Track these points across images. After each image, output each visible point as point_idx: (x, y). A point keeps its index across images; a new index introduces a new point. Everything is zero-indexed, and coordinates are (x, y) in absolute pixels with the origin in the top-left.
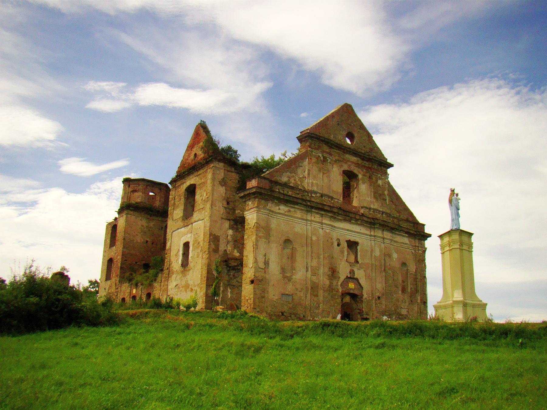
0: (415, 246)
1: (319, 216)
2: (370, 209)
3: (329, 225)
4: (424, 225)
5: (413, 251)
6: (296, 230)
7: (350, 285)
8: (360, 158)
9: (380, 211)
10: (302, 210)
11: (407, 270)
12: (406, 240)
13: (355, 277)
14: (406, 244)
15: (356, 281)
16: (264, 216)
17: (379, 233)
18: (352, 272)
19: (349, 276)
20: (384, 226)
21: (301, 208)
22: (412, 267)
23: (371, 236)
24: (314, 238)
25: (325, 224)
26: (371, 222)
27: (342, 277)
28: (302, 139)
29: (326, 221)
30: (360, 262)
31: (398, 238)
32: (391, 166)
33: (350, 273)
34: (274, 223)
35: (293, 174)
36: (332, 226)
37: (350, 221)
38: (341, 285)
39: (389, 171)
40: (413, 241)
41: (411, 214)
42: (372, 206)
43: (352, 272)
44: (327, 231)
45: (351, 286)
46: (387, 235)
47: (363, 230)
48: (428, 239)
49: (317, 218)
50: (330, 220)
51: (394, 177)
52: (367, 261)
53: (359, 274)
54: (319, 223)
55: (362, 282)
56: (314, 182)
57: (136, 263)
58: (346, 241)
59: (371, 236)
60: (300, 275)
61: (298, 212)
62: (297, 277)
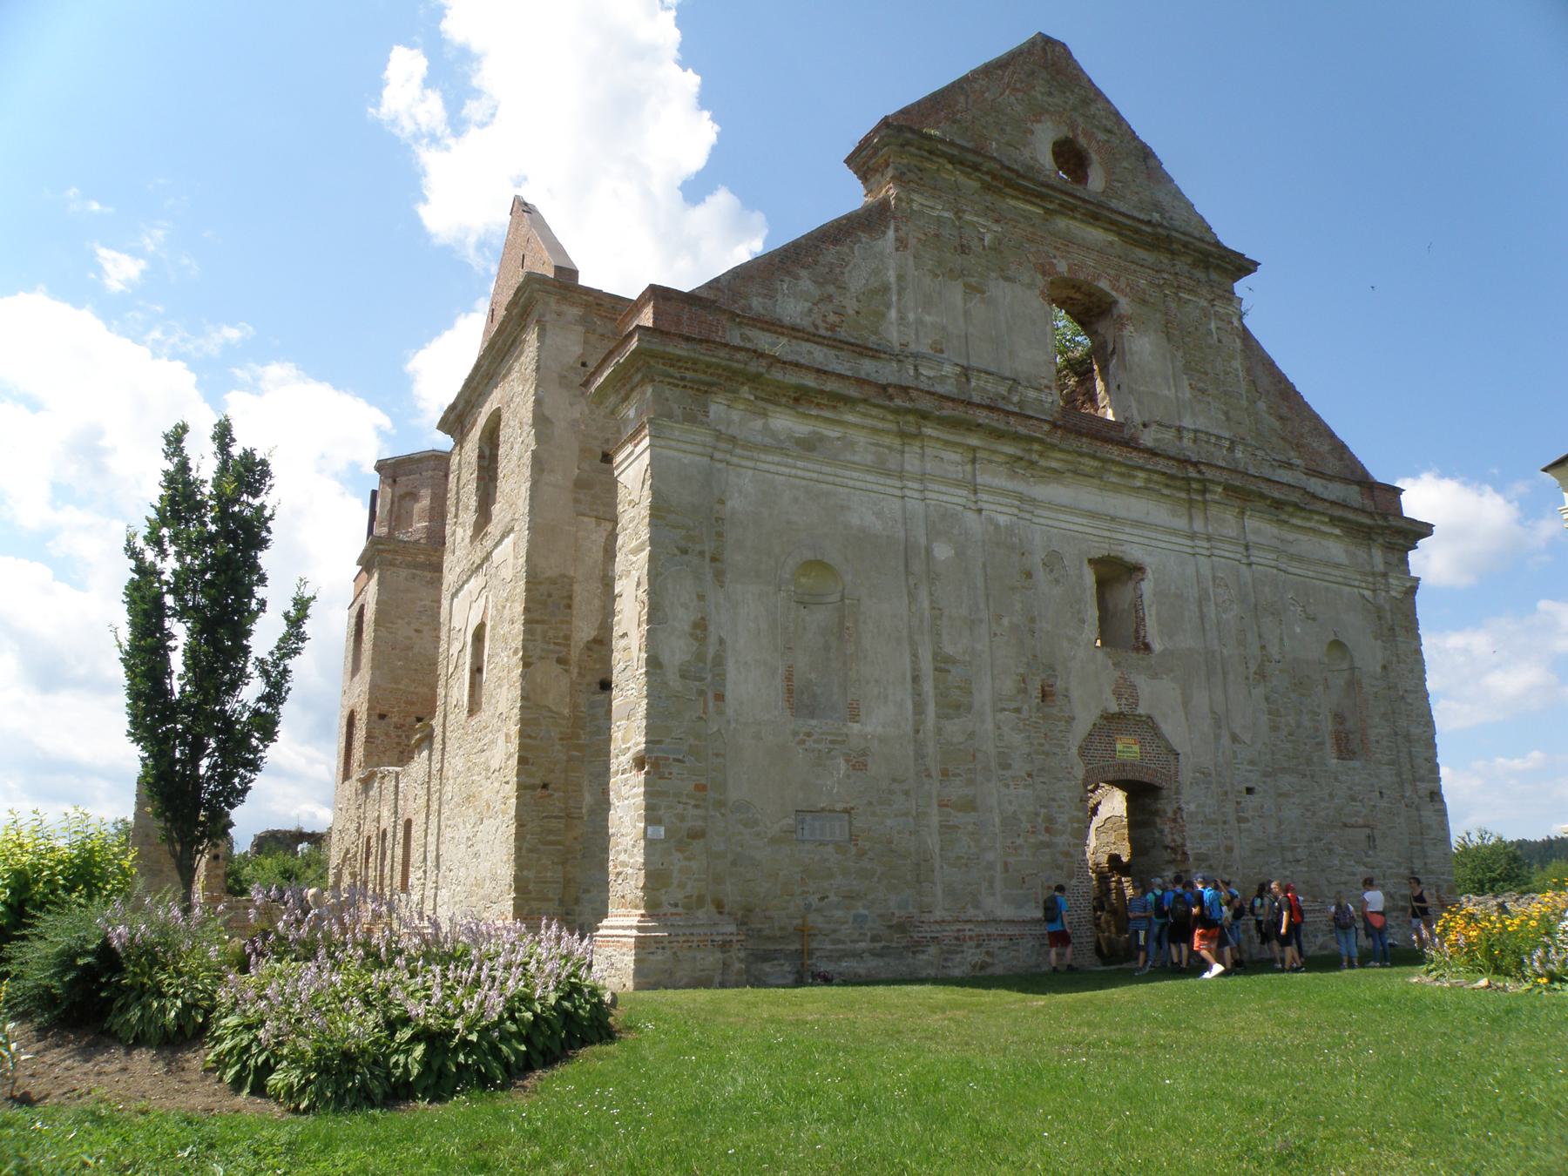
0: (1374, 574)
2: (1179, 430)
3: (1005, 493)
5: (1367, 593)
6: (855, 520)
7: (1119, 747)
8: (1119, 234)
9: (1219, 437)
10: (875, 431)
11: (1352, 669)
12: (1336, 548)
13: (1141, 710)
14: (1338, 566)
15: (1148, 727)
18: (1124, 690)
19: (1114, 708)
20: (1245, 494)
21: (869, 422)
22: (1369, 653)
23: (1193, 536)
24: (942, 552)
25: (992, 491)
26: (1186, 477)
27: (1085, 720)
28: (863, 161)
29: (993, 478)
30: (1157, 646)
31: (1306, 544)
32: (1243, 266)
33: (1119, 696)
34: (742, 486)
35: (831, 289)
36: (1021, 498)
37: (1101, 478)
38: (1083, 752)
39: (1241, 287)
40: (1361, 554)
41: (1341, 449)
42: (1187, 422)
43: (1124, 690)
44: (1002, 520)
45: (1128, 749)
46: (1260, 527)
47: (1155, 511)
48: (1421, 543)
50: (1013, 474)
51: (1262, 306)
53: (1157, 695)
54: (958, 484)
56: (928, 319)
58: (1090, 561)
60: (884, 718)
61: (861, 438)
62: (869, 729)
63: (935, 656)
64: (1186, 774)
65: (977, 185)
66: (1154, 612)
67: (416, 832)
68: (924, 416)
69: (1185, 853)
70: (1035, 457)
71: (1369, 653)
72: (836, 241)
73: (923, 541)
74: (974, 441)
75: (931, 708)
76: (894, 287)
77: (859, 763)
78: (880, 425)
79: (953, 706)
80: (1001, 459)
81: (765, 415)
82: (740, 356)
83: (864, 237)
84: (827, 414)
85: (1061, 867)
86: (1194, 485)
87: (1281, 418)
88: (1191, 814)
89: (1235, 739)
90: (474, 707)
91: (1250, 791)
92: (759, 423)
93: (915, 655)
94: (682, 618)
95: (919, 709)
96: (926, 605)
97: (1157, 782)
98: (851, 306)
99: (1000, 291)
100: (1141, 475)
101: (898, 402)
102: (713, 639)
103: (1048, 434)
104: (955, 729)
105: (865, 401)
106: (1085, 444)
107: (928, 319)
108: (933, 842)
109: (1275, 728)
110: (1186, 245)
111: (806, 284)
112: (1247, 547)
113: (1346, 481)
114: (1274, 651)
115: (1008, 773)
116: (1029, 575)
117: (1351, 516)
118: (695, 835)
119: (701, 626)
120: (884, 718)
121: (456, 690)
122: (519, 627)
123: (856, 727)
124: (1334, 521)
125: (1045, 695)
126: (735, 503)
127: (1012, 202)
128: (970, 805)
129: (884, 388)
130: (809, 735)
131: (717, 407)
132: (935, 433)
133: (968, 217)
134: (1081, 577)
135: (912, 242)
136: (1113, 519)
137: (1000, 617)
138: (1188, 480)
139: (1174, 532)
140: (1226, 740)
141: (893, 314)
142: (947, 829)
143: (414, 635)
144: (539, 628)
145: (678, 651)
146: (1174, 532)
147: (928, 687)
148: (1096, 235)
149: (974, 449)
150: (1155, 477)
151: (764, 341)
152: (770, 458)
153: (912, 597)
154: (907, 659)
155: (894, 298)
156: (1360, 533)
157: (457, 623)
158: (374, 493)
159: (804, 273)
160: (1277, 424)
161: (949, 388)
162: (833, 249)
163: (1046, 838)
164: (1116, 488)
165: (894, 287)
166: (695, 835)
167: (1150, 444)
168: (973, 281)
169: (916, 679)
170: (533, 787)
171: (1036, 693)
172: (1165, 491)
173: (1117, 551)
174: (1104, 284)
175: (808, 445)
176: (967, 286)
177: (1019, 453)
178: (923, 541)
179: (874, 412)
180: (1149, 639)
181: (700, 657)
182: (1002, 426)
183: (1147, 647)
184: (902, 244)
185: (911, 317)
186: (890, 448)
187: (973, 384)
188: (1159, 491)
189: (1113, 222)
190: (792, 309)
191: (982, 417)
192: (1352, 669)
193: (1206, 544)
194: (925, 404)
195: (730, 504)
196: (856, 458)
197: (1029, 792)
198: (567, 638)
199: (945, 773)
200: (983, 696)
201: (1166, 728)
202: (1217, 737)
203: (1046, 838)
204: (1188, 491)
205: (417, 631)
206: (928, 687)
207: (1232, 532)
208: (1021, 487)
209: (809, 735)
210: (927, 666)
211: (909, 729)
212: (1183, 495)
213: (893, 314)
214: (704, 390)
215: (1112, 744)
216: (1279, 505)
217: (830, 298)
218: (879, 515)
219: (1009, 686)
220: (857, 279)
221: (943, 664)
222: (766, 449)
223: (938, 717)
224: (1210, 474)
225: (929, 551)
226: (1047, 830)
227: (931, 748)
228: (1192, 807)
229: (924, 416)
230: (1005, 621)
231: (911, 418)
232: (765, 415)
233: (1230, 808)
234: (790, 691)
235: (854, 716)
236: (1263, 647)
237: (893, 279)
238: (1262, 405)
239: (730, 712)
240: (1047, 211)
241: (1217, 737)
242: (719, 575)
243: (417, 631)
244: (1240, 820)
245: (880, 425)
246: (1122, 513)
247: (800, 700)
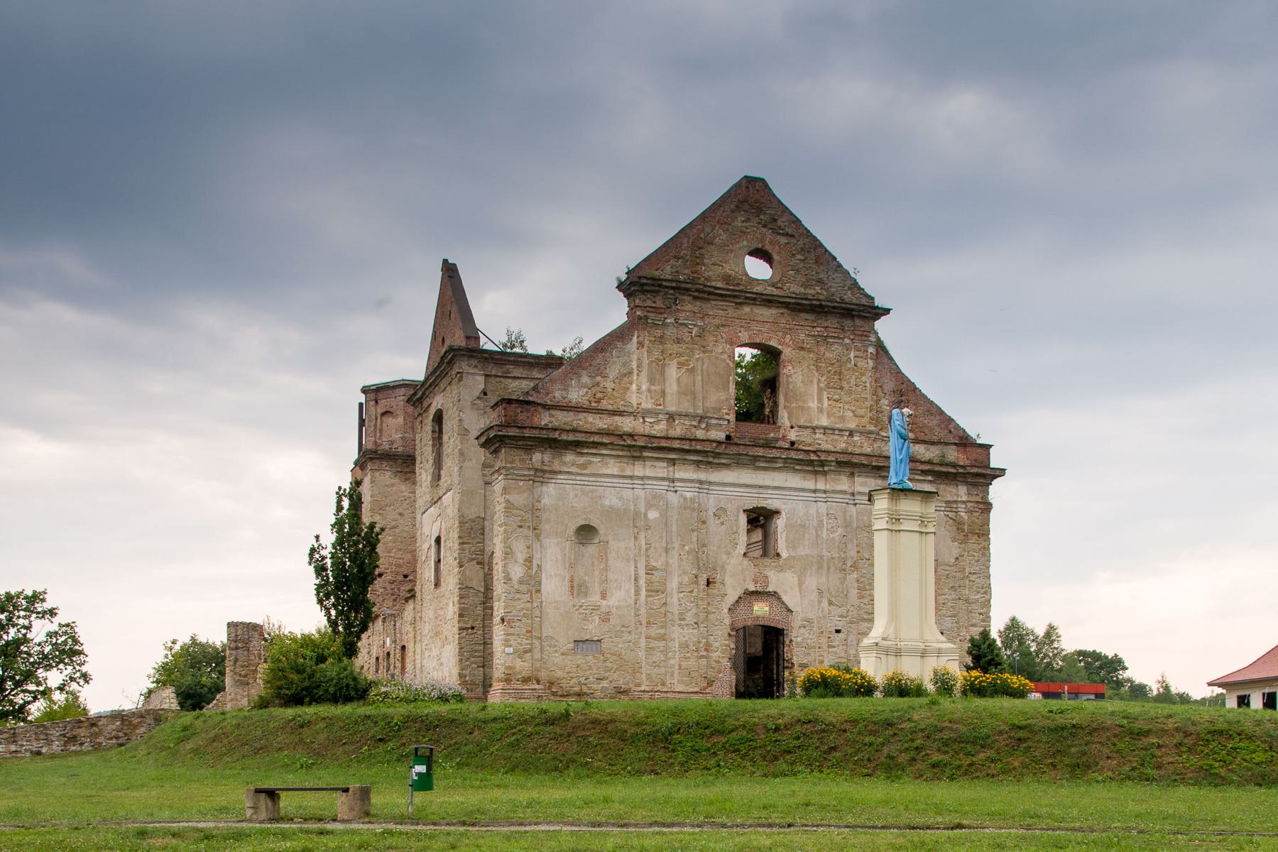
1: (665, 464)
4: (987, 447)
6: (607, 503)
7: (756, 608)
10: (618, 456)
13: (770, 589)
19: (752, 588)
24: (653, 515)
27: (733, 594)
30: (784, 554)
33: (756, 582)
36: (701, 482)
44: (688, 495)
45: (761, 609)
49: (661, 470)
52: (803, 551)
53: (780, 580)
57: (406, 576)
59: (815, 491)
61: (612, 461)
64: (796, 621)
66: (784, 536)
67: (409, 653)
72: (603, 350)
73: (643, 510)
75: (643, 593)
77: (605, 618)
83: (619, 345)
88: (797, 643)
89: (830, 603)
90: (437, 585)
91: (838, 631)
95: (637, 593)
96: (643, 542)
97: (780, 626)
101: (629, 442)
102: (535, 566)
104: (657, 601)
107: (653, 388)
111: (585, 379)
116: (704, 522)
117: (937, 468)
119: (529, 560)
121: (426, 573)
122: (456, 546)
123: (604, 603)
125: (708, 583)
128: (662, 638)
129: (621, 436)
134: (737, 520)
135: (647, 342)
140: (825, 604)
141: (634, 387)
142: (649, 650)
143: (398, 517)
147: (642, 582)
151: (561, 418)
154: (633, 568)
157: (426, 530)
158: (361, 405)
166: (526, 652)
169: (636, 579)
170: (467, 629)
171: (703, 582)
176: (679, 363)
178: (643, 510)
183: (778, 555)
184: (641, 344)
185: (644, 387)
191: (676, 445)
198: (483, 551)
199: (648, 623)
200: (673, 584)
201: (785, 598)
202: (820, 602)
205: (401, 514)
206: (642, 582)
208: (702, 476)
210: (642, 572)
213: (634, 387)
215: (751, 607)
217: (598, 384)
218: (620, 499)
221: (650, 571)
225: (646, 515)
226: (706, 650)
227: (643, 611)
228: (799, 639)
230: (687, 548)
233: (824, 640)
234: (572, 587)
241: (820, 602)
242: (538, 537)
243: (401, 514)
244: (830, 647)
247: (577, 588)
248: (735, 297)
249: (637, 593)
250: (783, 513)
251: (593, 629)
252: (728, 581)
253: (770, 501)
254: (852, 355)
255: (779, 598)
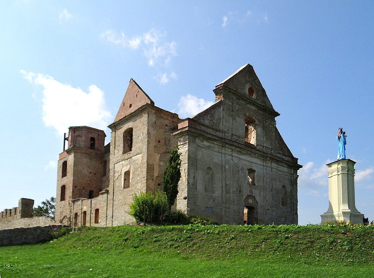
0: (291, 174)
2: (263, 146)
5: (290, 177)
9: (270, 148)
11: (286, 190)
12: (286, 169)
14: (285, 172)
15: (254, 198)
16: (193, 149)
17: (269, 164)
18: (251, 191)
19: (249, 194)
20: (273, 159)
21: (218, 144)
22: (289, 188)
23: (263, 166)
24: (227, 167)
27: (245, 196)
28: (217, 91)
30: (256, 185)
31: (281, 168)
35: (212, 118)
36: (239, 158)
37: (250, 155)
39: (276, 118)
40: (290, 170)
43: (251, 191)
45: (250, 201)
46: (274, 165)
47: (259, 162)
49: (229, 151)
50: (238, 154)
52: (261, 184)
53: (256, 193)
54: (230, 155)
55: (258, 198)
56: (227, 125)
58: (248, 169)
59: (263, 166)
60: (217, 194)
61: (216, 146)
62: (215, 195)
63: (225, 184)
65: (235, 98)
68: (226, 143)
69: (258, 219)
70: (241, 151)
71: (289, 188)
72: (214, 109)
74: (233, 148)
76: (222, 118)
78: (219, 144)
79: (228, 192)
80: (237, 151)
81: (203, 142)
82: (202, 132)
84: (212, 142)
85: (240, 219)
86: (265, 157)
87: (279, 144)
89: (267, 201)
91: (268, 210)
92: (202, 143)
93: (222, 184)
94: (192, 176)
95: (222, 192)
96: (224, 176)
98: (215, 121)
99: (238, 119)
100: (257, 155)
101: (223, 141)
102: (195, 179)
103: (245, 147)
105: (218, 140)
106: (249, 149)
108: (223, 213)
109: (273, 200)
110: (268, 110)
112: (272, 168)
113: (289, 157)
114: (274, 186)
115: (234, 203)
118: (193, 210)
119: (194, 177)
120: (217, 194)
123: (214, 194)
124: (286, 164)
125: (240, 191)
126: (199, 157)
127: (241, 101)
129: (221, 138)
130: (207, 195)
131: (197, 140)
132: (228, 146)
133: (234, 105)
136: (252, 162)
137: (234, 178)
138: (264, 156)
139: (261, 165)
140: (265, 201)
141: (221, 123)
142: (225, 211)
144: (149, 173)
145: (192, 181)
146: (261, 165)
147: (224, 189)
148: (254, 108)
149: (233, 149)
150: (259, 155)
151: (203, 128)
152: (204, 149)
153: (222, 174)
154: (221, 184)
155: (222, 120)
156: (290, 167)
159: (209, 115)
160: (279, 145)
161: (229, 138)
162: (213, 111)
163: (238, 214)
164: (252, 157)
165: (222, 118)
167: (258, 149)
168: (234, 117)
172: (260, 158)
173: (251, 168)
174: (254, 118)
175: (209, 147)
176: (233, 118)
177: (239, 150)
179: (219, 142)
180: (255, 183)
181: (194, 182)
182: (238, 146)
183: (255, 185)
184: (223, 109)
185: (224, 124)
186: (220, 148)
187: (233, 137)
188: (259, 158)
189: (257, 106)
190: (207, 122)
191: (235, 144)
192: (286, 190)
193: (265, 167)
194: (227, 141)
195: (198, 157)
196: (215, 150)
197: (237, 207)
202: (264, 200)
203: (238, 214)
204: (264, 158)
206: (224, 189)
207: (269, 166)
209: (207, 195)
211: (221, 195)
212: (263, 158)
213: (221, 123)
214: (195, 137)
215: (248, 200)
216: (278, 161)
218: (218, 160)
219: (235, 190)
220: (216, 117)
222: (203, 148)
223: (225, 194)
224: (268, 155)
227: (224, 199)
229: (226, 143)
230: (235, 179)
231: (224, 143)
232: (203, 142)
233: (265, 212)
235: (214, 193)
236: (272, 186)
237: (222, 116)
238: (277, 142)
239: (197, 190)
240: (246, 103)
241: (264, 200)
244: (266, 214)
245: (219, 144)
246: (253, 161)
247: (206, 190)
248: (246, 100)
249: (222, 192)
250: (256, 171)
251: (211, 203)
252: (244, 191)
253: (253, 167)
254: (271, 126)
255: (255, 198)
